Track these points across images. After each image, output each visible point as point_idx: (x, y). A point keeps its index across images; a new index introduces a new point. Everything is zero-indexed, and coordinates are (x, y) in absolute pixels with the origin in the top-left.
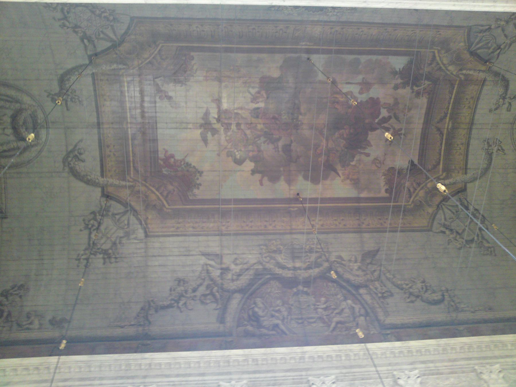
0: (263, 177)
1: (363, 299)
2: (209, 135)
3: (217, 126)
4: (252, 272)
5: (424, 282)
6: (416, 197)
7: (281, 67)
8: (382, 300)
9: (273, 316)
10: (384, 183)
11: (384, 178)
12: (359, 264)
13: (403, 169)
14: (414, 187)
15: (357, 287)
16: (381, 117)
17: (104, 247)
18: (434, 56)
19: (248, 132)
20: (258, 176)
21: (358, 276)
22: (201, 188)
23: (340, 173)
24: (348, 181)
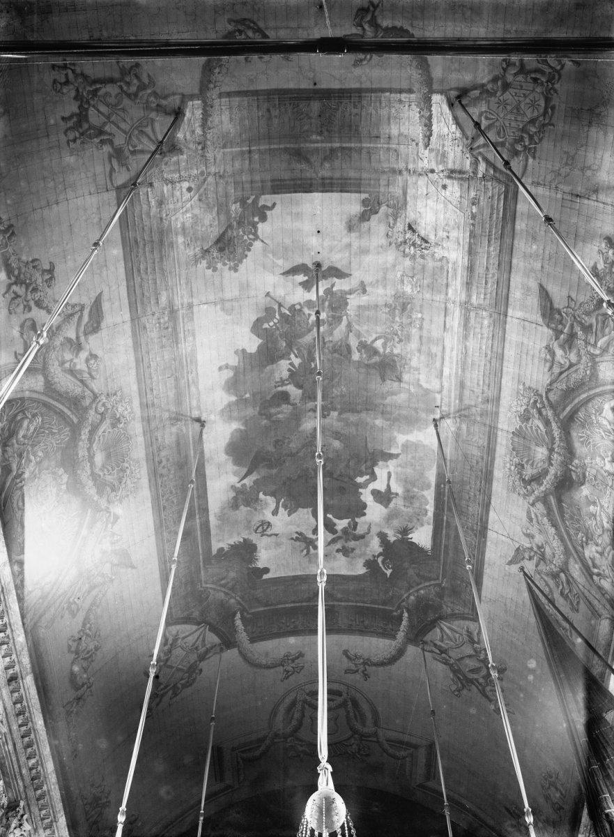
2: (301, 278)
16: (336, 521)
17: (92, 111)
18: (430, 579)
22: (210, 271)
23: (245, 481)
24: (232, 494)
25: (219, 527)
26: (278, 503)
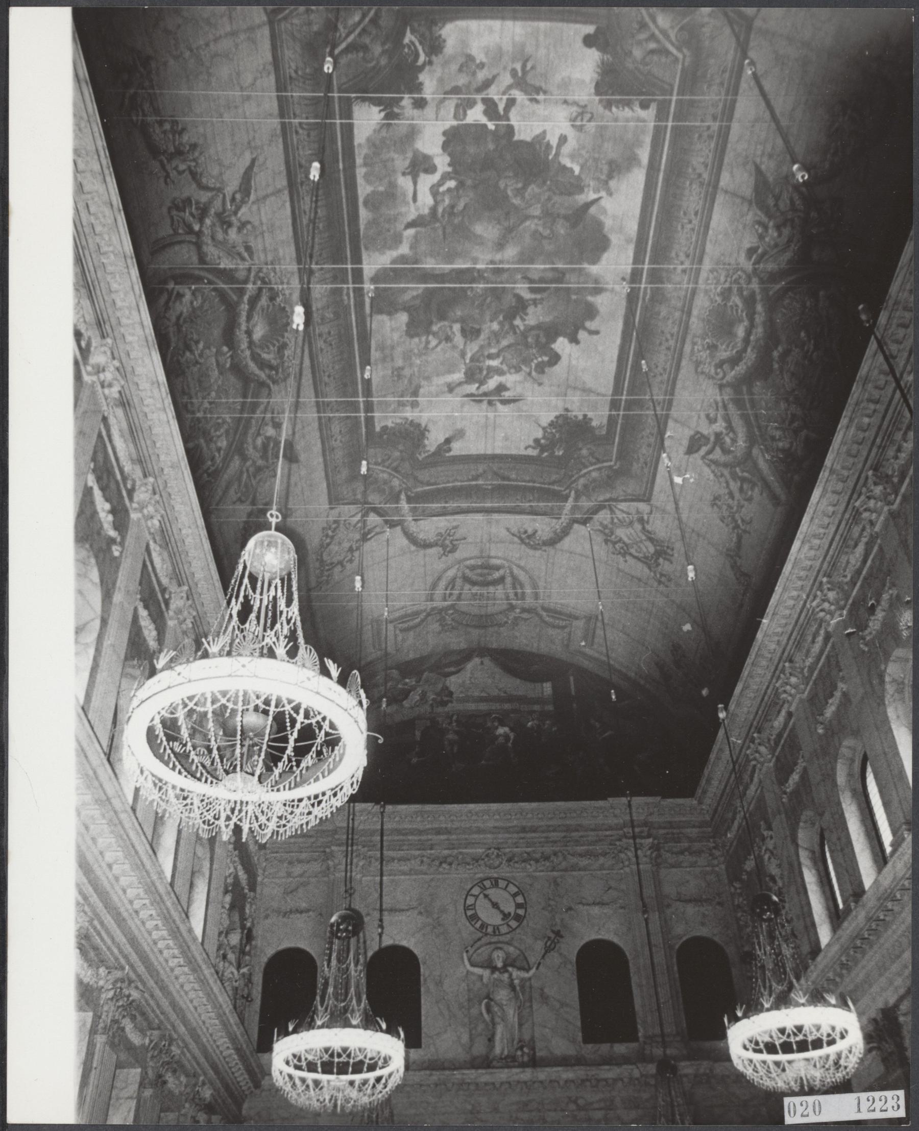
0: (585, 329)
2: (507, 395)
3: (492, 384)
4: (730, 406)
6: (667, 36)
7: (390, 314)
10: (627, 109)
11: (617, 107)
13: (603, 63)
14: (647, 40)
16: (484, 120)
19: (504, 343)
20: (582, 335)
23: (592, 196)
24: (612, 183)
25: (639, 143)
26: (557, 154)
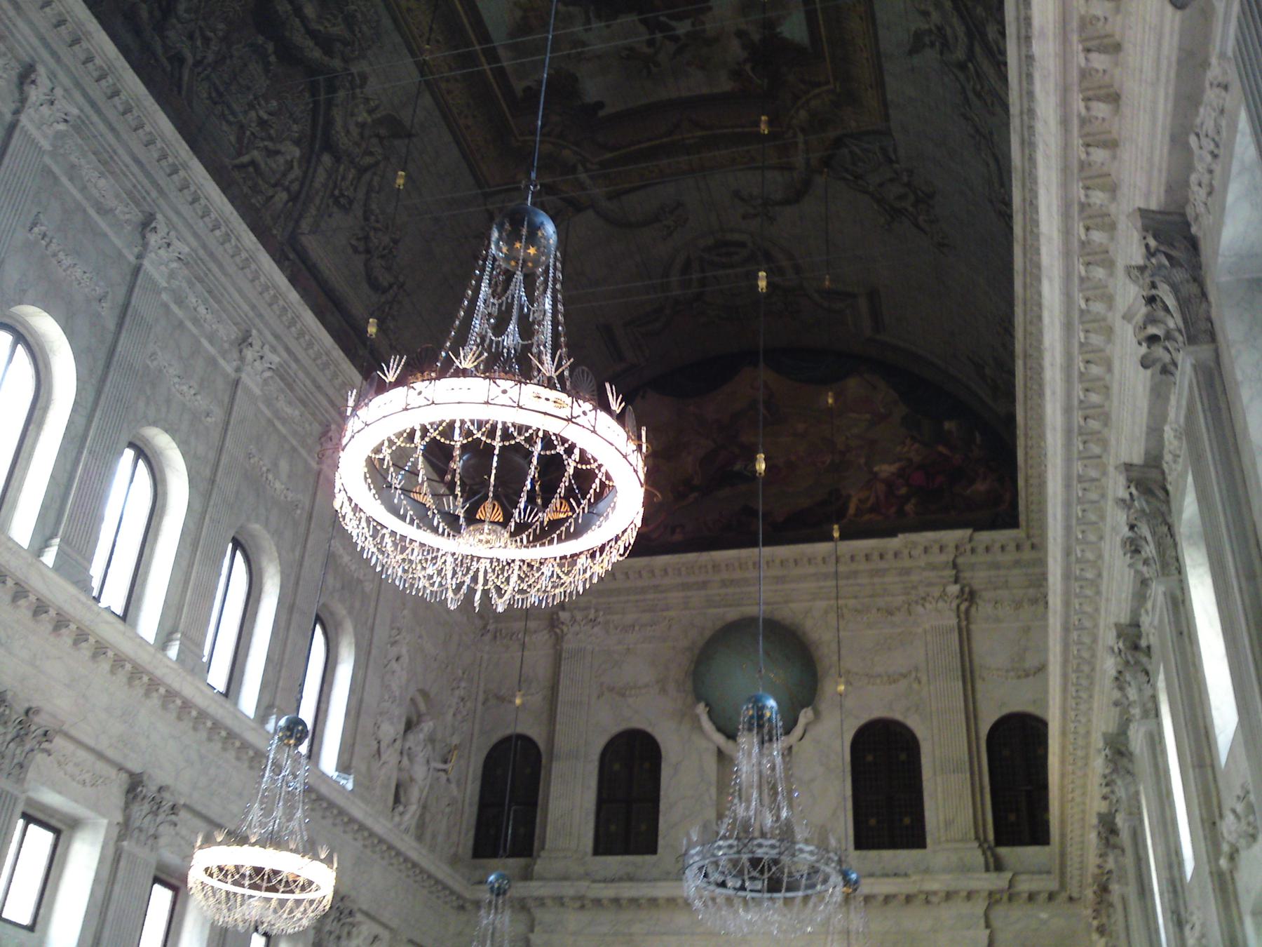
1: (315, 171)
5: (395, 242)
8: (331, 201)
9: (191, 37)
12: (369, 120)
15: (329, 146)
18: (818, 85)
21: (348, 132)
24: (519, 14)
